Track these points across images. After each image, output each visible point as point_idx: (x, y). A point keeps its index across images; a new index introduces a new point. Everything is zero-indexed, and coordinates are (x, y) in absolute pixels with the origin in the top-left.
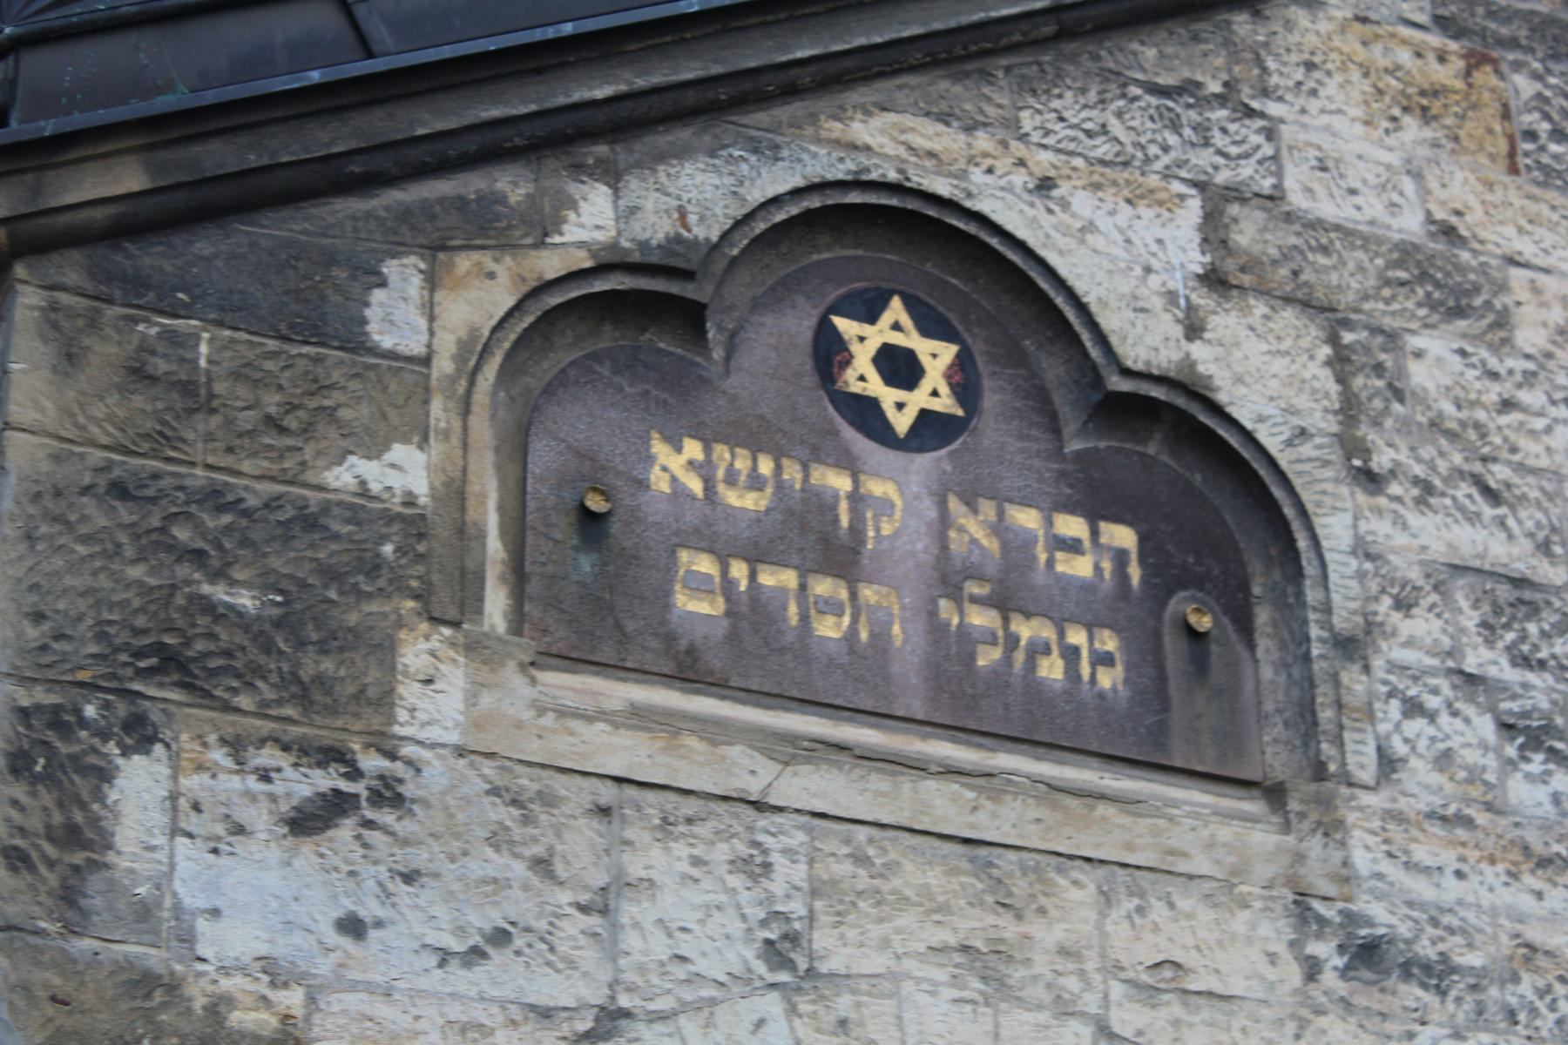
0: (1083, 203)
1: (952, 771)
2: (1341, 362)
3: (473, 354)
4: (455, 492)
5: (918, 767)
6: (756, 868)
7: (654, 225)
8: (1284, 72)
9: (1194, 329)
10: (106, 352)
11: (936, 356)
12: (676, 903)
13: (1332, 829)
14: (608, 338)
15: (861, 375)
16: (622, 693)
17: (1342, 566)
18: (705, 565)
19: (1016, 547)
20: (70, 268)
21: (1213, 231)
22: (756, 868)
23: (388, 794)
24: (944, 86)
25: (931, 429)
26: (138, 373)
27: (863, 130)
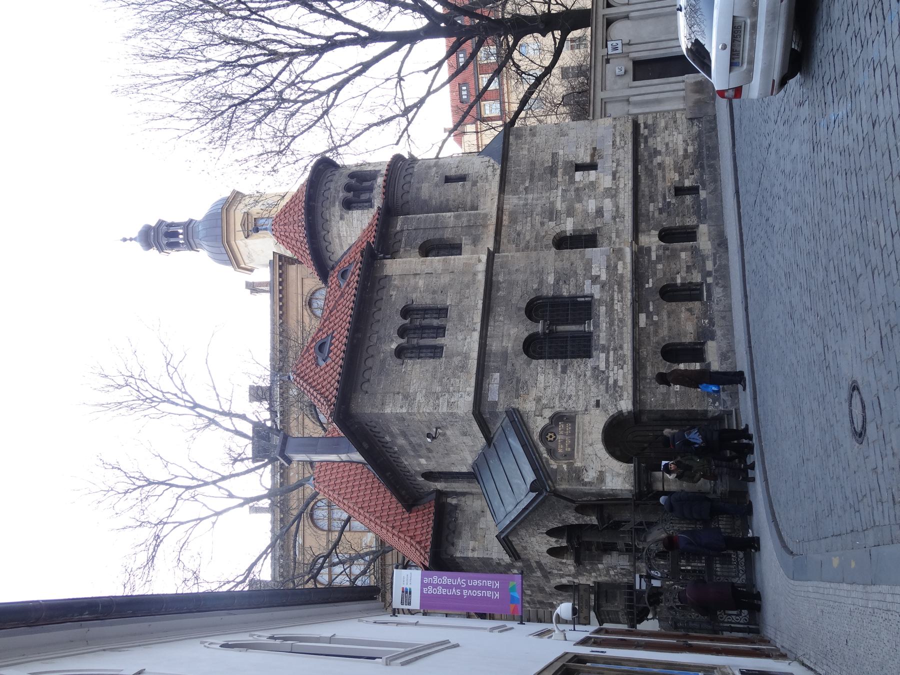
0: (537, 424)
1: (578, 434)
2: (546, 408)
3: (556, 463)
4: (565, 464)
5: (578, 437)
6: (586, 447)
7: (545, 452)
8: (524, 410)
9: (545, 418)
10: (560, 483)
11: (550, 434)
12: (589, 451)
13: (578, 411)
14: (552, 454)
15: (552, 439)
16: (576, 454)
17: (560, 409)
18: (566, 449)
19: (562, 430)
20: (555, 485)
21: (538, 416)
22: (586, 447)
23: (585, 467)
24: (531, 433)
25: (555, 435)
26: (561, 481)
27: (535, 439)
